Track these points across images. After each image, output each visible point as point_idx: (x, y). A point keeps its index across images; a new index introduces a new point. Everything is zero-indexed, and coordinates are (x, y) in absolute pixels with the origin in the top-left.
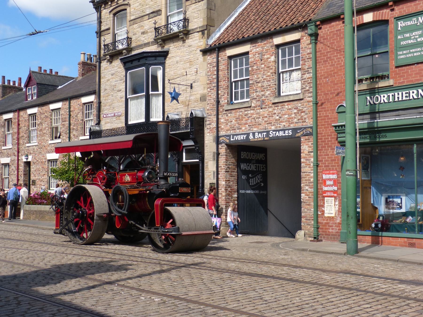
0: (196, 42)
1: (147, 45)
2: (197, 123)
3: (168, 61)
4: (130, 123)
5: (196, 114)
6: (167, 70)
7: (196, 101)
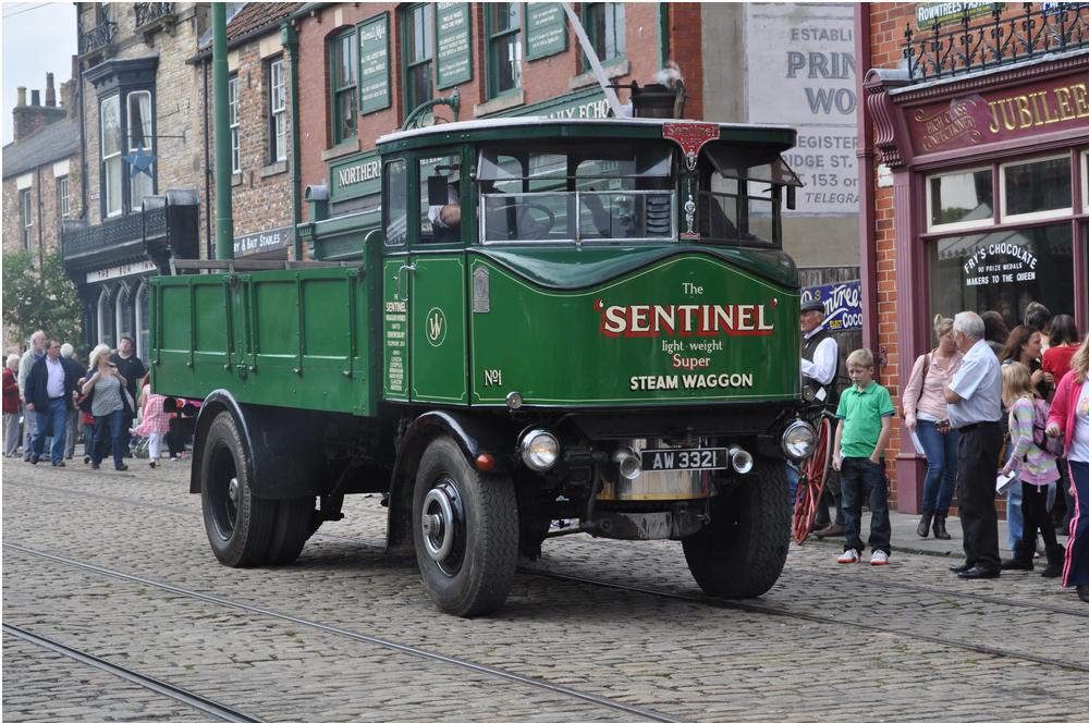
0: (187, 42)
1: (131, 41)
2: (182, 219)
3: (162, 79)
4: (110, 215)
5: (173, 201)
6: (158, 99)
7: (189, 170)
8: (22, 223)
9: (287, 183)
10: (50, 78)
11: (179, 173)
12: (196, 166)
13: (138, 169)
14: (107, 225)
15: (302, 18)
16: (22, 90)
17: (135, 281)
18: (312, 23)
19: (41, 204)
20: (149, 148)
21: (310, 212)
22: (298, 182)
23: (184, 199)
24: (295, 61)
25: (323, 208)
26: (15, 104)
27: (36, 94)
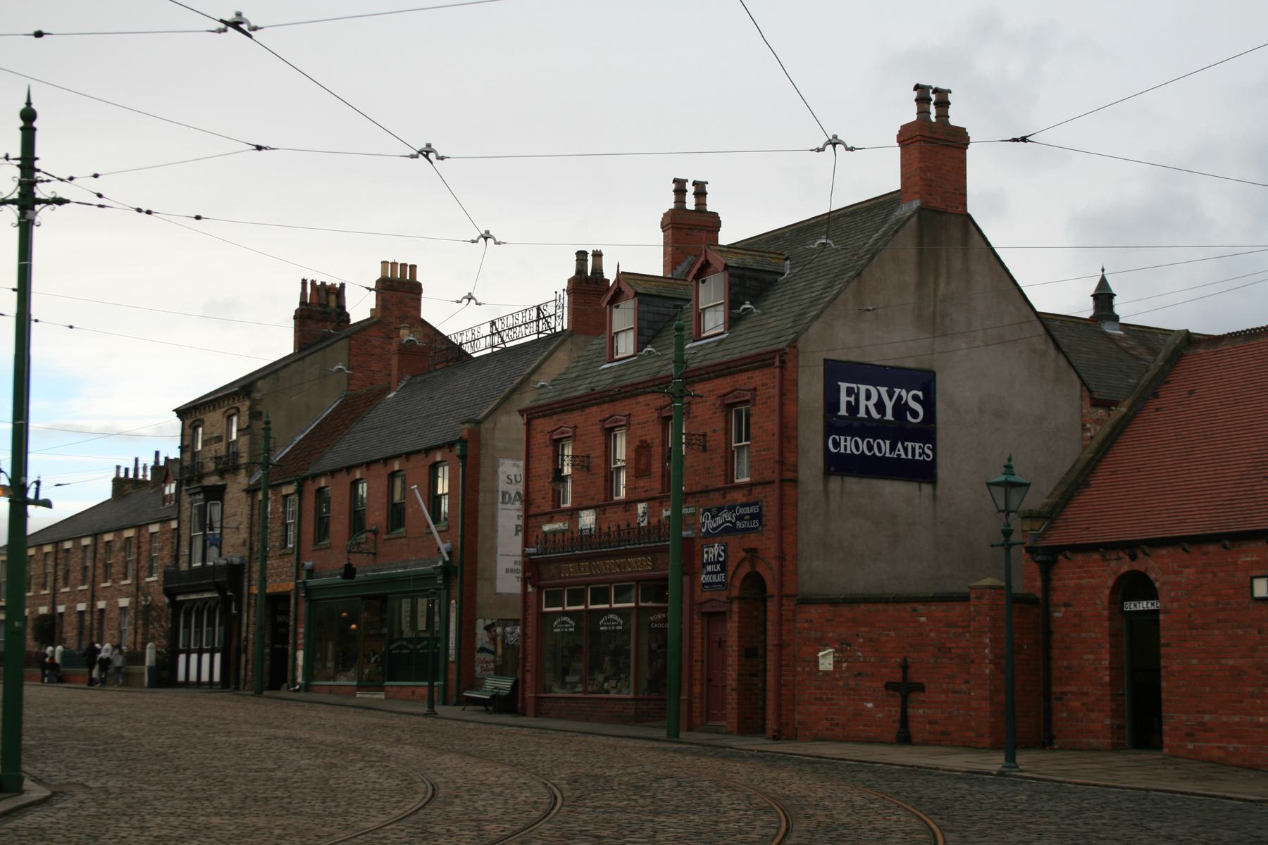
0: (242, 480)
1: (211, 474)
2: (235, 573)
3: (227, 497)
8: (125, 557)
9: (293, 558)
10: (137, 460)
11: (233, 549)
12: (244, 544)
13: (212, 544)
14: (192, 571)
15: (304, 479)
16: (118, 467)
17: (206, 600)
18: (310, 482)
19: (139, 548)
20: (218, 531)
21: (304, 575)
22: (298, 559)
23: (236, 561)
24: (300, 499)
25: (311, 573)
26: (114, 476)
27: (127, 470)
